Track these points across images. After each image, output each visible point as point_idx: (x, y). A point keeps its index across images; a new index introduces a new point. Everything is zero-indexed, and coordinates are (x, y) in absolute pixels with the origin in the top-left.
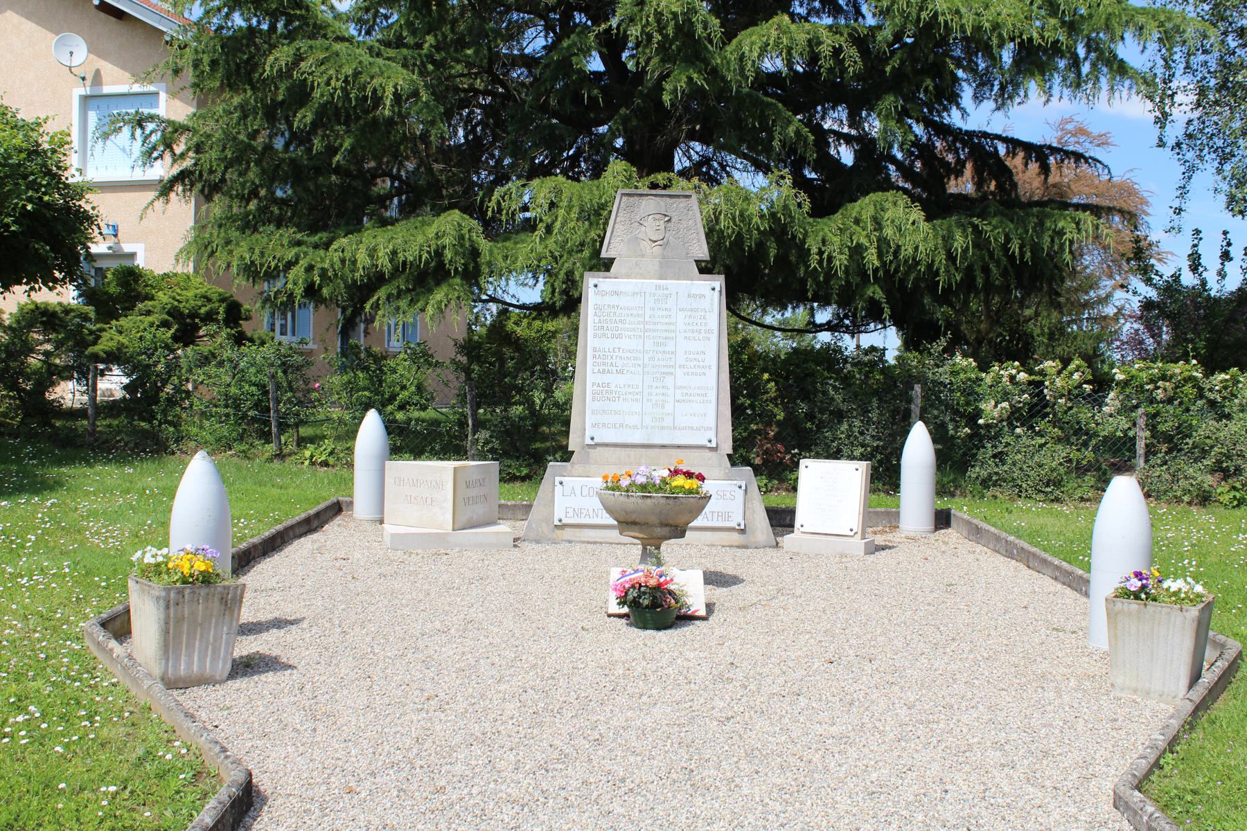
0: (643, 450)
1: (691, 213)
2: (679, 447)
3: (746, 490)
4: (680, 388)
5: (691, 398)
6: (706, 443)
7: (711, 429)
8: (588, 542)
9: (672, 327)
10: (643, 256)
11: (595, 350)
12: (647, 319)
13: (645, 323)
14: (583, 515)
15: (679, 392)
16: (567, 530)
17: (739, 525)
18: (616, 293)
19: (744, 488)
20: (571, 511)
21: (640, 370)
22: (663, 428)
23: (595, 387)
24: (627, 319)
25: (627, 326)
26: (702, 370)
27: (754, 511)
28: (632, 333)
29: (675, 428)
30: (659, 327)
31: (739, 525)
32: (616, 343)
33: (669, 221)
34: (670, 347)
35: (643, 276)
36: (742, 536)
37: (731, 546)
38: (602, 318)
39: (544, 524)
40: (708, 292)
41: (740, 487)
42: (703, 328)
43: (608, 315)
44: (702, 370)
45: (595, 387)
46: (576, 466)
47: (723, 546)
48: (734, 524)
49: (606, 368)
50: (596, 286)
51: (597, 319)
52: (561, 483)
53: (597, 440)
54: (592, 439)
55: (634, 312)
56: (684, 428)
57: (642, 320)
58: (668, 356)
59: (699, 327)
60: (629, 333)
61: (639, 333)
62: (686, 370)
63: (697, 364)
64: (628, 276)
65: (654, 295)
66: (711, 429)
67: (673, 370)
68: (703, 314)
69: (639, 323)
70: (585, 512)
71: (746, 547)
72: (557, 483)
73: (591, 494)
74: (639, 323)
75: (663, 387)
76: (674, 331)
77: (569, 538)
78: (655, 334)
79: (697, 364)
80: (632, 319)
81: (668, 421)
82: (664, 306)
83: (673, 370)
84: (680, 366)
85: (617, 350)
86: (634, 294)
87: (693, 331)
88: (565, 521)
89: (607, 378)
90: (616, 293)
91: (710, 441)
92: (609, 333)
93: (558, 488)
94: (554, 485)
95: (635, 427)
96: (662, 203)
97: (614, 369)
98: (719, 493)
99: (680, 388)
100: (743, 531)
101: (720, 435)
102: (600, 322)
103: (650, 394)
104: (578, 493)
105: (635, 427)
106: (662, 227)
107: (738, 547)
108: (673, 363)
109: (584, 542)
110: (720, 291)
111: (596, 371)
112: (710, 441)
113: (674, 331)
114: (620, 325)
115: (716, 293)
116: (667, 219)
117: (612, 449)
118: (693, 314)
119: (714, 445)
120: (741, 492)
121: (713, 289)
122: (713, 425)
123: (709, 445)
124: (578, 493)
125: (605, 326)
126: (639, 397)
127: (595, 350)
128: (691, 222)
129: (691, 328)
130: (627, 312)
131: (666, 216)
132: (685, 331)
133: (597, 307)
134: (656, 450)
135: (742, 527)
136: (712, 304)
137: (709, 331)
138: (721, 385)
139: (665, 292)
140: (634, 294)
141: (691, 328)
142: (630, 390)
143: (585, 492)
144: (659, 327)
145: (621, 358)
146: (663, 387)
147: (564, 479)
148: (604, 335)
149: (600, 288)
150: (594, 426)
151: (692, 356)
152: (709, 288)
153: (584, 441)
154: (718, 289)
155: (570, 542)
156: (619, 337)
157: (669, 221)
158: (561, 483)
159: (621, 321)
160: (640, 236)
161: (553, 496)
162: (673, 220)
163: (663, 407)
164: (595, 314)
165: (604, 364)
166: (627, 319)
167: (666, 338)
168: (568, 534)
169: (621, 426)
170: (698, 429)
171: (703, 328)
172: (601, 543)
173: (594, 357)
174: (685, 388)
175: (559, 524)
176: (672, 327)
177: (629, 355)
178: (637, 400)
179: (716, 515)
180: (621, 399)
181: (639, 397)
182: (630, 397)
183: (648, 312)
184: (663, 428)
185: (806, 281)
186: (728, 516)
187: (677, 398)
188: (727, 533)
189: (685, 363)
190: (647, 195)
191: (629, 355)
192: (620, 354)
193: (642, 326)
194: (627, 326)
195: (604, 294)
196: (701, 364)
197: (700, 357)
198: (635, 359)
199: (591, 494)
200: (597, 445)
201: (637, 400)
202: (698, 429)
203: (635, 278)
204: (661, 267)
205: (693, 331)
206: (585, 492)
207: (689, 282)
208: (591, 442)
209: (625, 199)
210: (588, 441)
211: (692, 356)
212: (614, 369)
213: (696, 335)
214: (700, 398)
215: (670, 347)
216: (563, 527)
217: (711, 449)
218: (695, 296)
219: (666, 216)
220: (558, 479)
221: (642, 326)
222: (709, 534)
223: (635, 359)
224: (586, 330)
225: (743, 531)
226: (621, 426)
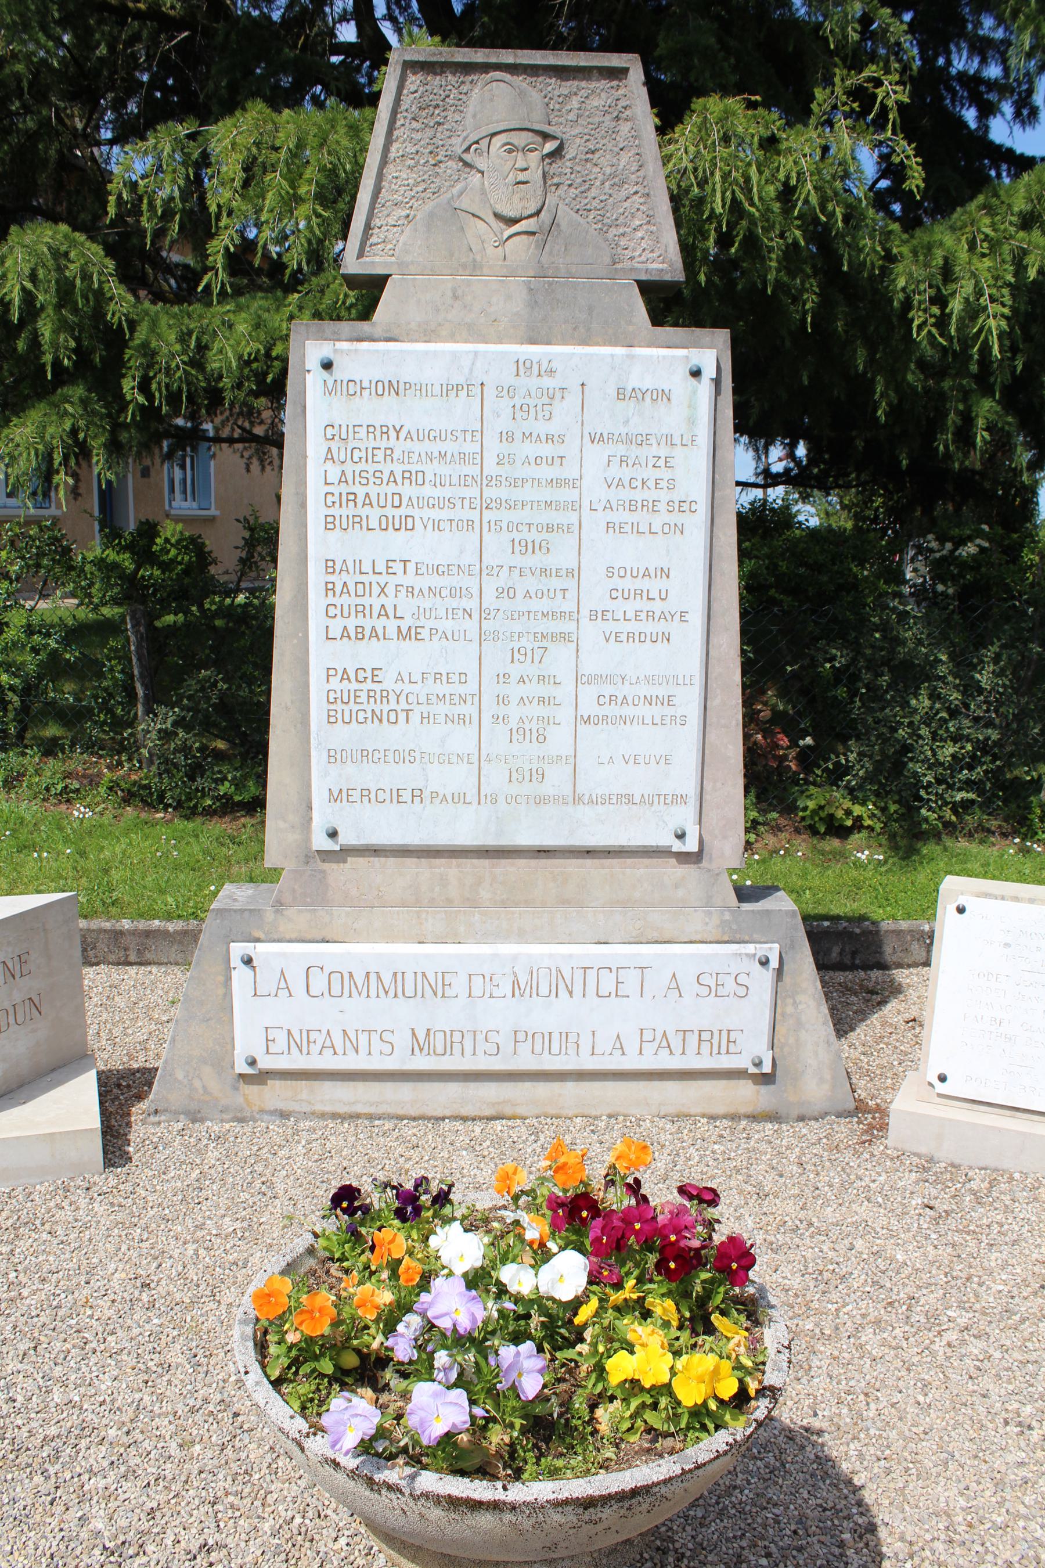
0: (484, 864)
1: (625, 128)
2: (589, 853)
3: (780, 972)
4: (594, 679)
5: (628, 711)
6: (666, 840)
7: (683, 799)
8: (335, 1116)
9: (569, 495)
10: (475, 268)
11: (330, 565)
12: (491, 467)
13: (483, 481)
14: (315, 1049)
15: (588, 694)
16: (275, 1085)
17: (758, 1064)
18: (393, 388)
19: (774, 963)
20: (281, 1038)
21: (471, 626)
22: (540, 800)
23: (335, 683)
24: (430, 469)
25: (428, 491)
26: (661, 627)
27: (799, 1025)
28: (445, 514)
29: (577, 799)
30: (527, 493)
31: (758, 1064)
32: (397, 544)
33: (557, 154)
34: (563, 555)
35: (474, 333)
36: (763, 1089)
37: (734, 1117)
38: (349, 468)
39: (207, 1071)
40: (678, 382)
41: (764, 963)
42: (663, 496)
43: (370, 455)
44: (661, 627)
45: (335, 683)
46: (291, 912)
47: (713, 1118)
48: (743, 1062)
49: (368, 624)
50: (327, 366)
51: (334, 474)
52: (248, 961)
53: (347, 838)
54: (333, 834)
55: (450, 447)
56: (606, 800)
57: (475, 470)
58: (556, 583)
59: (651, 495)
60: (435, 514)
61: (468, 514)
62: (611, 627)
63: (644, 605)
64: (429, 334)
65: (511, 392)
66: (683, 799)
67: (570, 627)
68: (663, 452)
69: (464, 481)
70: (320, 1039)
71: (773, 1117)
72: (235, 961)
73: (336, 989)
74: (464, 481)
75: (542, 678)
76: (575, 506)
77: (281, 1105)
78: (515, 516)
79: (644, 605)
80: (443, 470)
81: (557, 780)
82: (541, 428)
83: (570, 627)
84: (593, 616)
85: (398, 567)
86: (450, 389)
87: (632, 506)
88: (265, 1063)
89: (370, 654)
90: (393, 388)
91: (681, 836)
92: (374, 514)
93: (241, 975)
94: (229, 969)
95: (459, 799)
96: (535, 96)
97: (392, 625)
98: (705, 980)
99: (592, 680)
100: (767, 1079)
101: (712, 816)
102: (343, 480)
103: (502, 700)
104: (298, 985)
105: (459, 799)
106: (535, 175)
107: (754, 1118)
108: (569, 606)
109: (323, 1116)
110: (717, 382)
111: (336, 631)
112: (681, 836)
113: (575, 506)
114: (407, 490)
115: (705, 388)
116: (550, 146)
117: (391, 861)
118: (634, 451)
119: (691, 845)
120: (767, 977)
121: (696, 373)
122: (690, 787)
123: (677, 846)
124: (298, 985)
125: (361, 491)
126: (469, 709)
127: (330, 565)
128: (625, 158)
129: (626, 494)
130: (427, 446)
131: (546, 136)
132: (609, 507)
133: (333, 433)
134: (522, 862)
135: (767, 1068)
136: (691, 421)
137: (683, 506)
138: (715, 671)
139: (547, 382)
140: (450, 389)
141: (626, 494)
142: (443, 689)
143: (319, 983)
144: (527, 493)
145: (410, 590)
146: (542, 678)
147: (261, 950)
148: (357, 521)
149: (340, 372)
150: (335, 797)
151: (628, 584)
152: (683, 371)
153: (308, 840)
154: (709, 372)
155: (284, 1115)
156: (405, 524)
157: (557, 154)
158: (248, 961)
159: (408, 477)
160: (465, 203)
161: (228, 995)
162: (570, 152)
163: (542, 738)
164: (329, 456)
165: (361, 610)
166: (430, 469)
167: (549, 528)
168: (275, 1094)
169: (417, 795)
170: (647, 801)
171: (663, 496)
172: (371, 1117)
173: (329, 588)
174: (608, 679)
175: (249, 1071)
176: (569, 495)
177: (436, 581)
178: (462, 719)
179: (693, 1040)
180: (415, 717)
181: (469, 709)
182: (442, 709)
183: (493, 447)
184: (540, 800)
185: (873, 381)
186: (728, 1041)
187: (585, 711)
188: (722, 1083)
189: (610, 605)
190: (486, 68)
191: (436, 581)
192: (410, 579)
193: (474, 492)
194: (428, 491)
195: (353, 389)
196: (657, 606)
197: (654, 586)
198: (457, 592)
199: (336, 989)
200: (347, 852)
201: (462, 719)
202: (647, 801)
203: (452, 338)
204: (533, 304)
205: (632, 506)
206: (319, 983)
207: (620, 351)
208: (328, 845)
209: (414, 81)
210: (321, 842)
211: (628, 584)
212: (392, 625)
213: (642, 517)
214: (657, 711)
215: (563, 555)
216: (263, 1077)
217: (684, 858)
218: (639, 395)
219: (546, 136)
220: (238, 949)
221: (474, 492)
222: (672, 1088)
223: (457, 592)
224: (303, 505)
225: (767, 1079)
226: (417, 795)
